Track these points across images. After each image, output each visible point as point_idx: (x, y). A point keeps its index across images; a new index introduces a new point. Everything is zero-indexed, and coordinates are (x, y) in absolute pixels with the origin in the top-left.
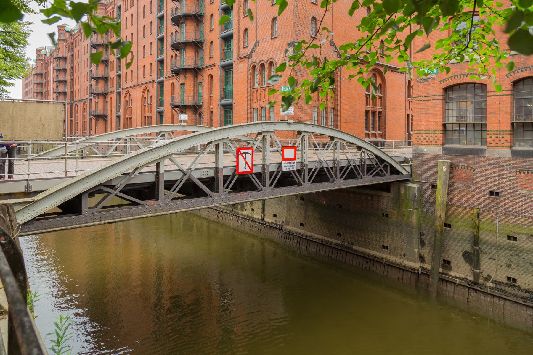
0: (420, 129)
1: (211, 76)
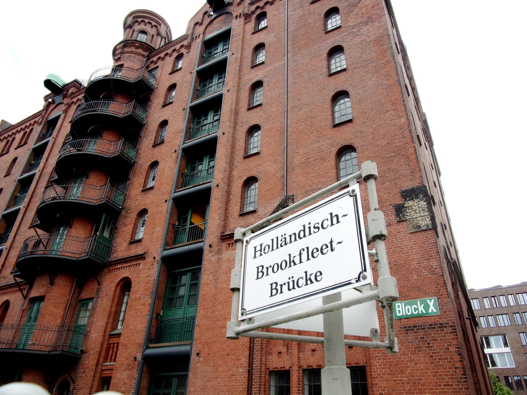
1: (126, 285)
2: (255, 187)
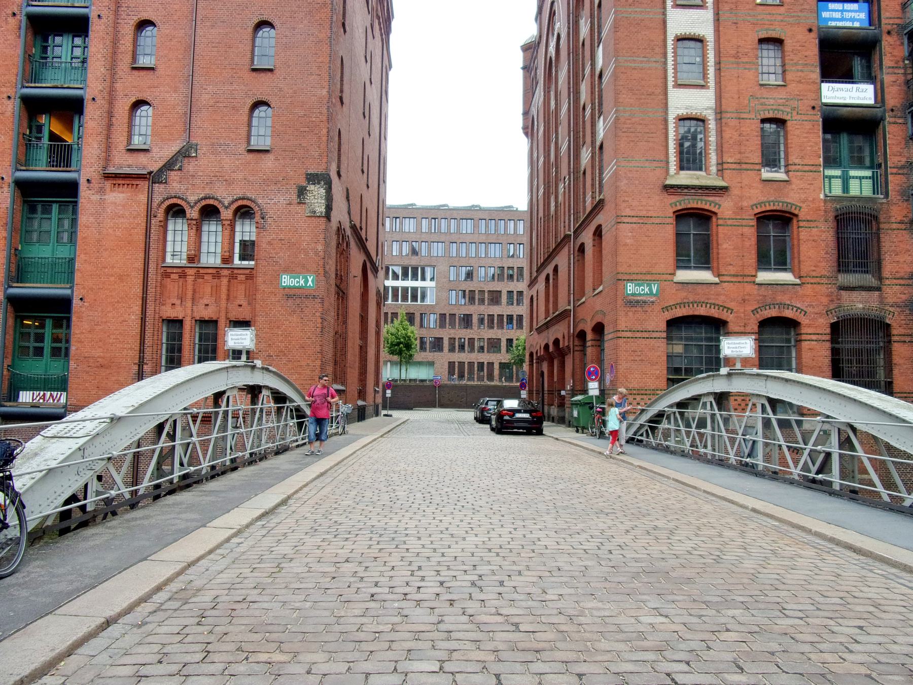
0: (631, 386)
2: (144, 110)
